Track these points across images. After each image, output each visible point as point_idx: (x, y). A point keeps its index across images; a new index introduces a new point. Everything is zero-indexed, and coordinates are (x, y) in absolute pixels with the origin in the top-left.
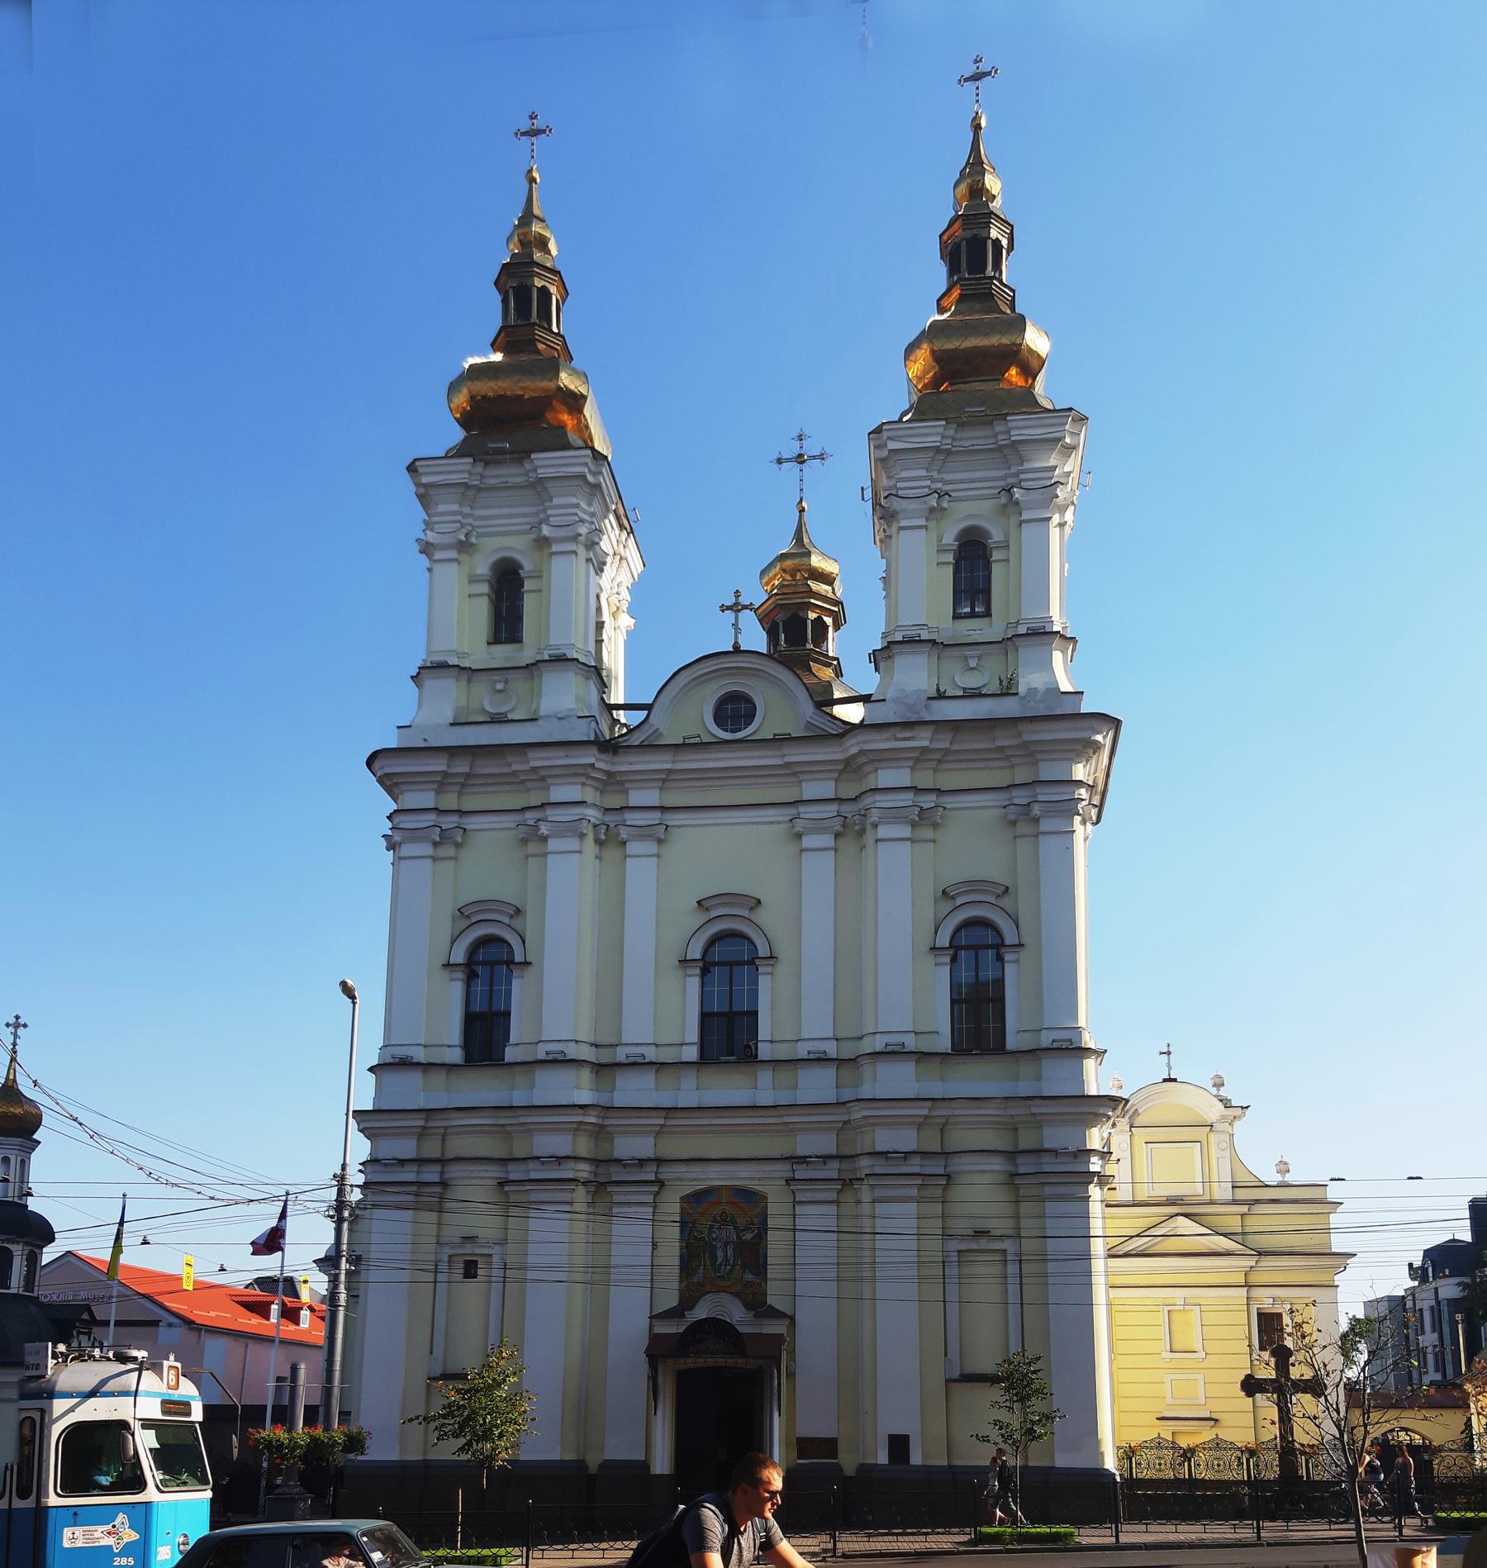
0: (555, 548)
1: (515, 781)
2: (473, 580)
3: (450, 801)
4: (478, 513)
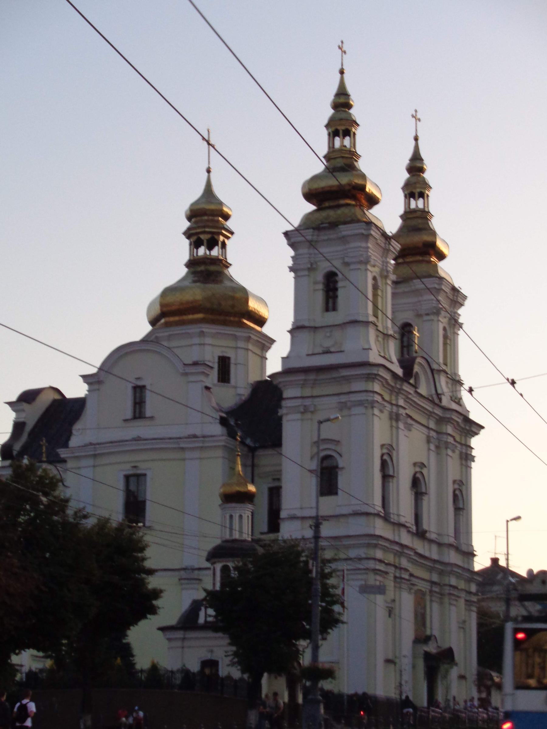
3: (307, 392)
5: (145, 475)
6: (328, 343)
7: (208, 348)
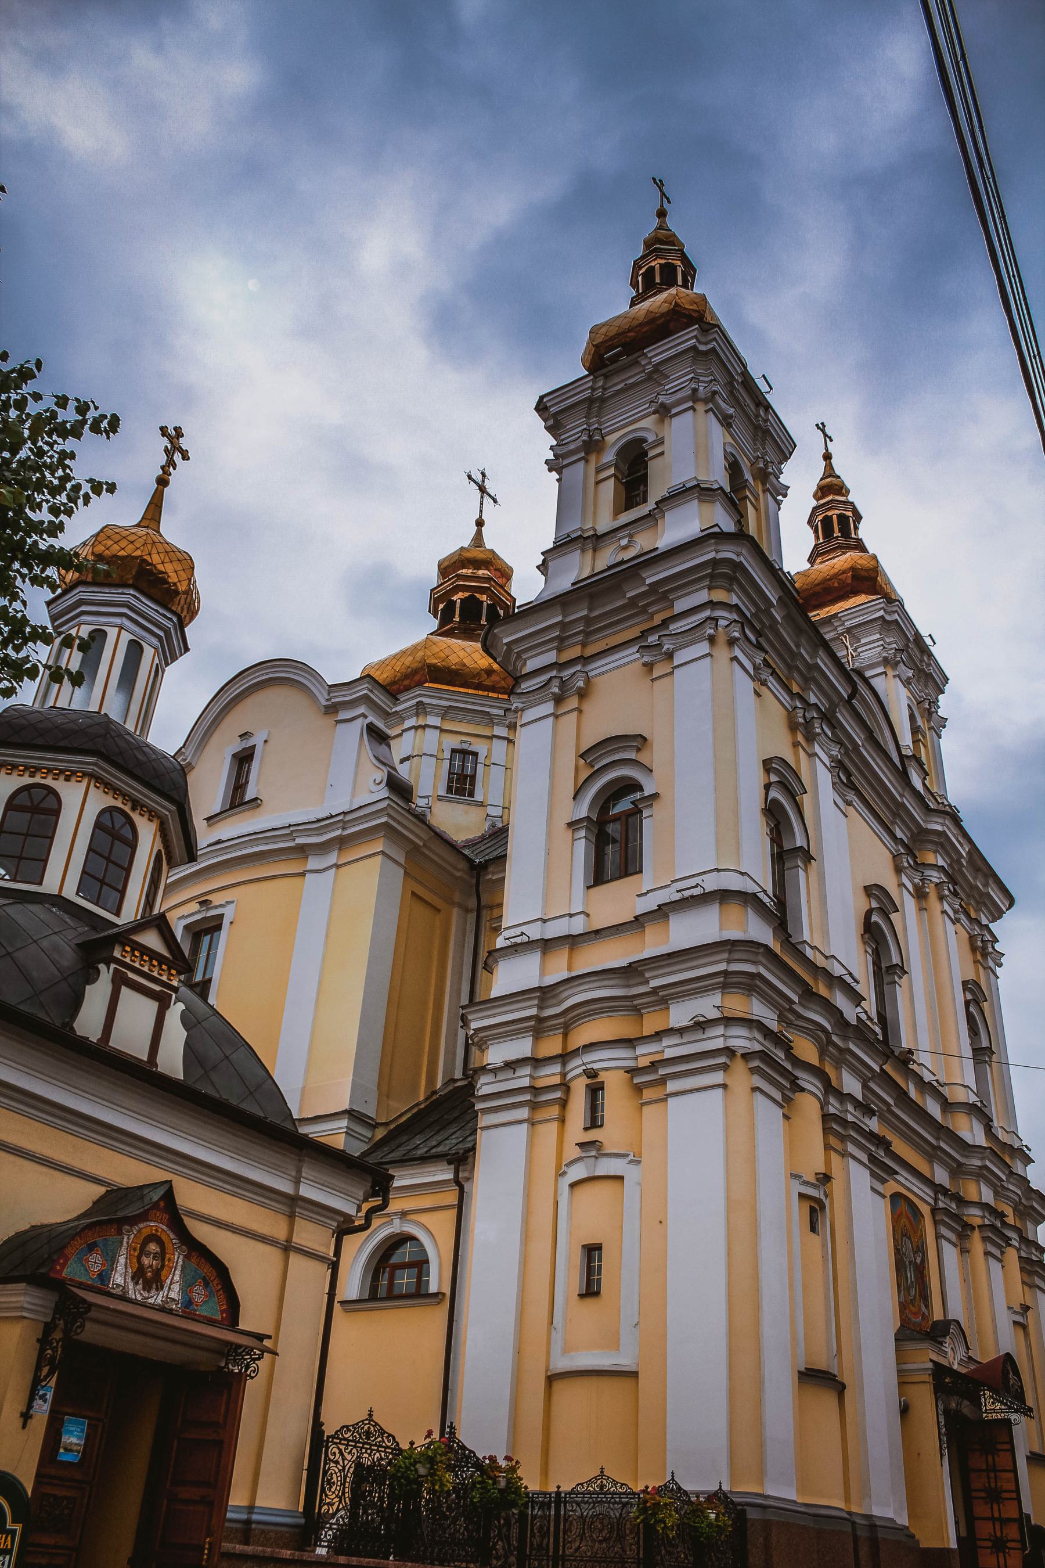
0: (673, 411)
7: (432, 735)
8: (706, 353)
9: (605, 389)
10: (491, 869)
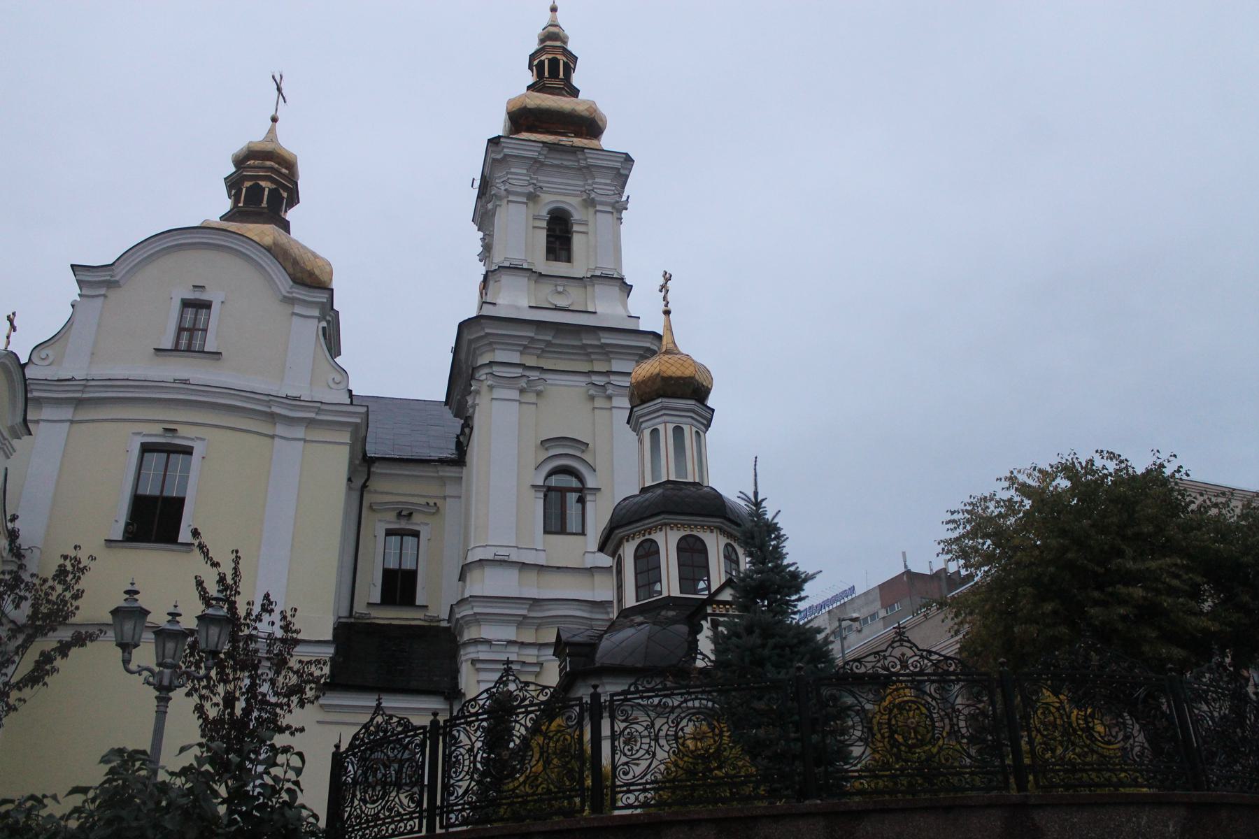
0: (599, 208)
1: (586, 352)
2: (536, 218)
3: (531, 361)
4: (540, 178)
5: (188, 451)
6: (561, 302)
8: (621, 175)
9: (546, 158)
10: (377, 464)
